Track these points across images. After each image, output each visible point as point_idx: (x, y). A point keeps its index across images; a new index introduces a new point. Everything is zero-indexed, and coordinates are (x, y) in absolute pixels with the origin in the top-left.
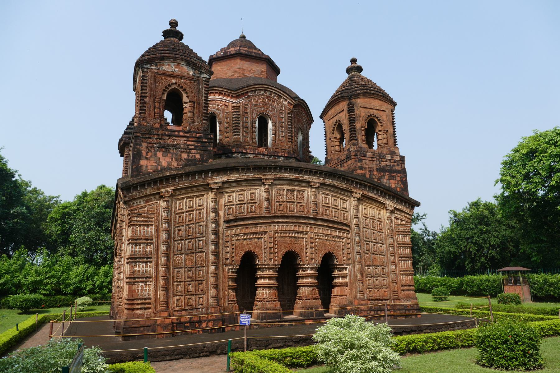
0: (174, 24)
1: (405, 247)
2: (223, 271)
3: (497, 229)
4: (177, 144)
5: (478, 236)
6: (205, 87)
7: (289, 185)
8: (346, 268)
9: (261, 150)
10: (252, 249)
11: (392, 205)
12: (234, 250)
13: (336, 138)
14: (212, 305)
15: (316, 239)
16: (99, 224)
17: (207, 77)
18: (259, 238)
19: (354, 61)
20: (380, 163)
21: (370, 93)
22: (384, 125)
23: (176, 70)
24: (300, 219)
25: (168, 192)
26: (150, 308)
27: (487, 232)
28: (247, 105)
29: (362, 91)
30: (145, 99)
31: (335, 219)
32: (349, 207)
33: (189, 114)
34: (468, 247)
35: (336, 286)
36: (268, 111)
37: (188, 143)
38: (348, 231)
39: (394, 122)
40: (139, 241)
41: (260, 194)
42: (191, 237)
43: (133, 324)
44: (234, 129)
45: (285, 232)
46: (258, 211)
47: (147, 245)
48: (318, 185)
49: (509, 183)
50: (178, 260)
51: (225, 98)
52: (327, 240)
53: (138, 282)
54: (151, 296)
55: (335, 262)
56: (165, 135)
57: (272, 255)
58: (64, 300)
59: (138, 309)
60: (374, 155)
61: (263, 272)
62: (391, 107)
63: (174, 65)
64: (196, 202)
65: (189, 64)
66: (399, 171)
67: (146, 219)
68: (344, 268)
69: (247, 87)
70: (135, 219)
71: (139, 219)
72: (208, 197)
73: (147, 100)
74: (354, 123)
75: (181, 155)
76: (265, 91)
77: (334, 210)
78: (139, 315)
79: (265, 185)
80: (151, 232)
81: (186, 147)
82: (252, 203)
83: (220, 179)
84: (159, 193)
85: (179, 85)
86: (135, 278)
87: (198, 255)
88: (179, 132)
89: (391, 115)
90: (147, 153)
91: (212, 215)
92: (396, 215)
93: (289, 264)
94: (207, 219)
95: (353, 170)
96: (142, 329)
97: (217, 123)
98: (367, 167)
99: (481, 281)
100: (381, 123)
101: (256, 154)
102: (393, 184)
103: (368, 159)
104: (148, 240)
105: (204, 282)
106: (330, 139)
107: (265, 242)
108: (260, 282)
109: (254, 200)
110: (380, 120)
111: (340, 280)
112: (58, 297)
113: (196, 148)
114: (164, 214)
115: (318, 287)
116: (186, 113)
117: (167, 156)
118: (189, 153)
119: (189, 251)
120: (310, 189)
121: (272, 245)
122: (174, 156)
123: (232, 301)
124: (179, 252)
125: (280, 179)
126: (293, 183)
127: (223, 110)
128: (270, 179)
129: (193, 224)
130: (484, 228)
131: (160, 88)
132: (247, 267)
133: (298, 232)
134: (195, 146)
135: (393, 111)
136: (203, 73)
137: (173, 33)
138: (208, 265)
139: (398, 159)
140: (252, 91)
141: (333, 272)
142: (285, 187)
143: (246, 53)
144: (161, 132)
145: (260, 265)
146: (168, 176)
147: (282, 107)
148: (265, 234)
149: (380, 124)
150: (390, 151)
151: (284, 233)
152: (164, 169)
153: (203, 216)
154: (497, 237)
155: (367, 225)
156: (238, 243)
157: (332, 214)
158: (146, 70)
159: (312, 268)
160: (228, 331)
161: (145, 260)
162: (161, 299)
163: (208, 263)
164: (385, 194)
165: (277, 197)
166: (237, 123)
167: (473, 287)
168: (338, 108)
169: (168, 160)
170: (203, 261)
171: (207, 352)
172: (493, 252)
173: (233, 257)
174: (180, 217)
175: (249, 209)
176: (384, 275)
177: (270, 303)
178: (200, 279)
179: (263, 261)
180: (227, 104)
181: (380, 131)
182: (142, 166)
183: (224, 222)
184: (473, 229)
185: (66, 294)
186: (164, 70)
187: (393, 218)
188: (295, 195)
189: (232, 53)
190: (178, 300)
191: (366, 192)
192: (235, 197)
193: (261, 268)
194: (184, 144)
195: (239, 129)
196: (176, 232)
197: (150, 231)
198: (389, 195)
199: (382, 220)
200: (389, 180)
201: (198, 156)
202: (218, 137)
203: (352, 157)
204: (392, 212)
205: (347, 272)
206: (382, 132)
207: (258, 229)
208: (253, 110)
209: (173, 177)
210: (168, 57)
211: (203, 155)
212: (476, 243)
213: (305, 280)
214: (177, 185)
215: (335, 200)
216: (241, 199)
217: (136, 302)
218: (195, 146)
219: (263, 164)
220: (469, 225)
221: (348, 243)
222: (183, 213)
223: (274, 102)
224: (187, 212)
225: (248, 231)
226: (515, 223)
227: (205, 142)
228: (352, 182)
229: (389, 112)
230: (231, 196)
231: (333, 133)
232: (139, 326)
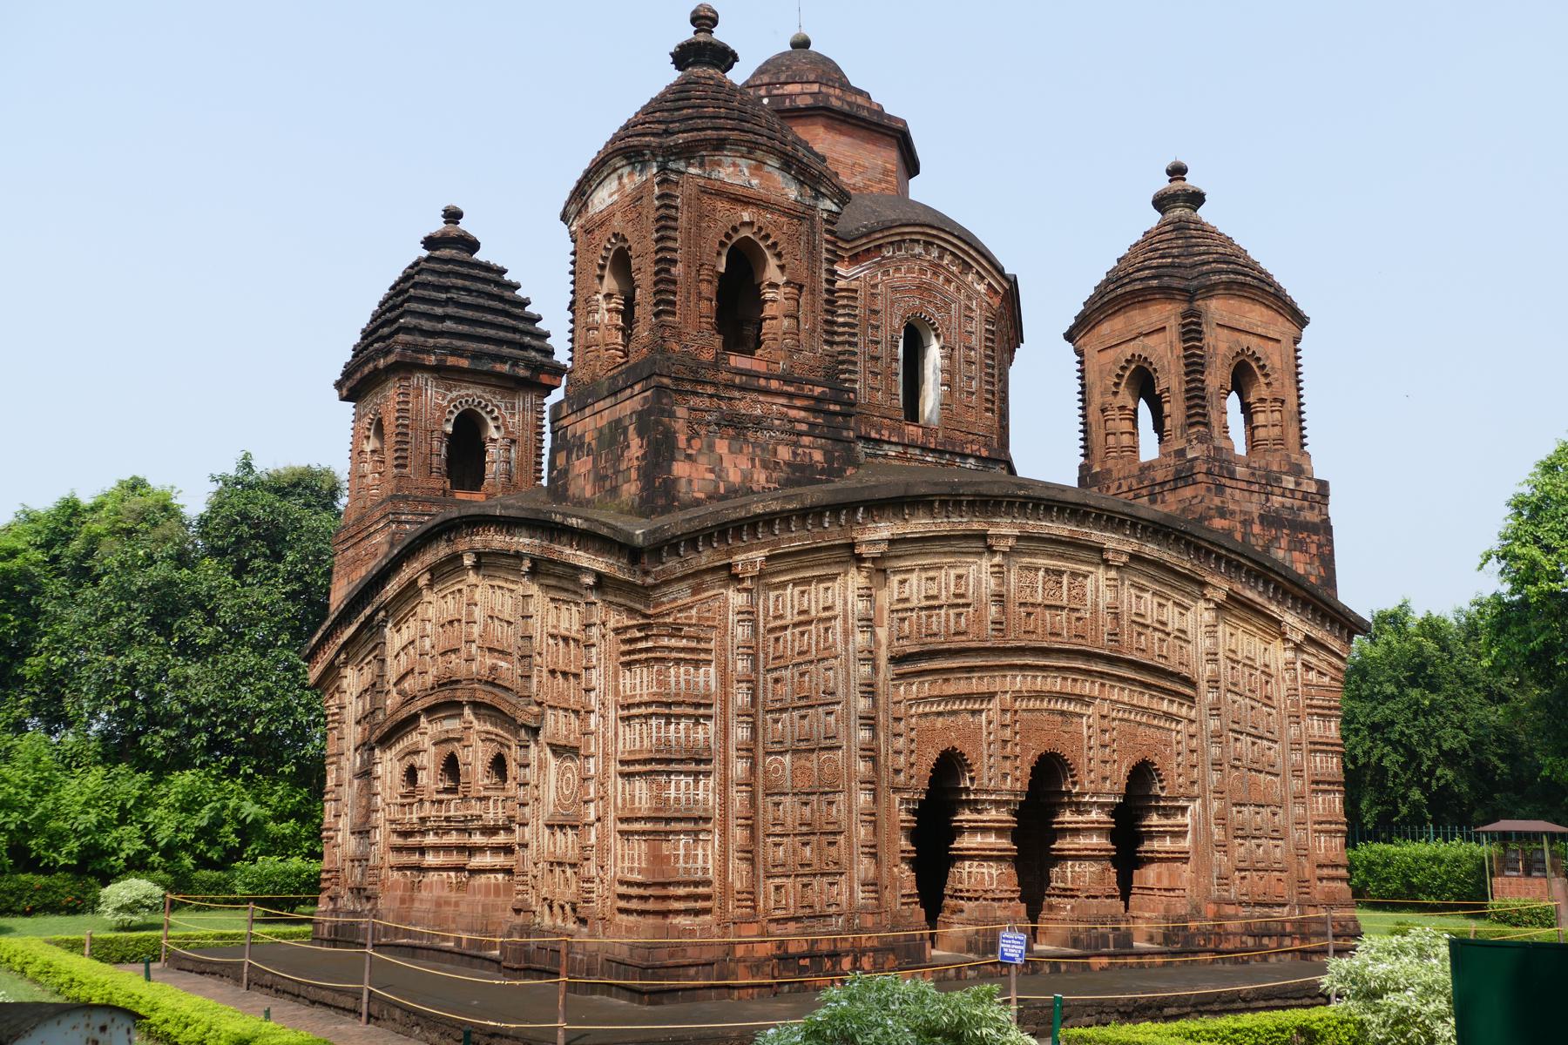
0: (704, 20)
1: (1326, 752)
2: (889, 809)
3: (1460, 700)
5: (1407, 720)
6: (827, 241)
7: (1051, 556)
8: (1184, 809)
9: (912, 430)
10: (956, 744)
11: (1299, 625)
12: (913, 747)
13: (1122, 408)
14: (865, 907)
16: (161, 621)
17: (834, 208)
18: (974, 712)
20: (1267, 500)
21: (1244, 284)
22: (1276, 384)
23: (755, 182)
24: (1075, 659)
25: (753, 563)
26: (707, 911)
27: (1434, 709)
28: (875, 286)
31: (1161, 663)
32: (1195, 630)
33: (786, 322)
34: (1377, 753)
35: (1152, 860)
36: (931, 309)
37: (793, 413)
38: (1191, 699)
39: (1298, 374)
40: (675, 710)
41: (979, 581)
42: (806, 704)
43: (671, 956)
45: (1039, 695)
46: (974, 629)
47: (697, 723)
48: (1125, 559)
49: (1534, 565)
50: (776, 770)
52: (1140, 724)
53: (677, 833)
54: (710, 875)
55: (1156, 790)
56: (735, 387)
58: (46, 889)
59: (678, 912)
61: (979, 812)
62: (1293, 330)
63: (749, 167)
64: (816, 598)
66: (1314, 524)
67: (694, 644)
69: (881, 231)
70: (665, 642)
71: (673, 642)
73: (678, 270)
75: (775, 453)
76: (927, 244)
77: (1158, 635)
78: (684, 932)
80: (706, 683)
81: (788, 426)
82: (958, 606)
83: (884, 530)
84: (729, 565)
85: (760, 229)
86: (668, 820)
87: (825, 755)
90: (689, 440)
91: (861, 639)
92: (1305, 656)
94: (847, 650)
95: (1202, 518)
96: (692, 971)
98: (1237, 508)
99: (1416, 860)
100: (1266, 375)
101: (904, 445)
102: (1301, 565)
104: (698, 705)
105: (841, 839)
106: (1103, 411)
107: (990, 723)
108: (966, 842)
111: (1168, 844)
112: (23, 877)
114: (741, 632)
115: (1113, 860)
118: (796, 444)
119: (803, 745)
120: (1101, 570)
121: (1008, 733)
124: (777, 747)
125: (1030, 538)
126: (1061, 549)
128: (1006, 537)
129: (811, 662)
130: (1423, 696)
131: (713, 236)
134: (811, 425)
135: (1297, 341)
136: (824, 195)
138: (850, 788)
140: (892, 243)
141: (1142, 817)
142: (1041, 561)
143: (846, 107)
145: (976, 791)
146: (760, 515)
147: (969, 298)
149: (1262, 380)
150: (1290, 463)
152: (732, 492)
153: (834, 645)
154: (1461, 727)
155: (1235, 685)
156: (924, 723)
157: (1151, 648)
158: (673, 177)
159: (1101, 806)
161: (693, 767)
162: (738, 886)
163: (849, 781)
165: (1021, 589)
166: (850, 344)
167: (1386, 880)
168: (1142, 318)
170: (836, 775)
172: (1450, 774)
173: (912, 765)
174: (777, 639)
175: (952, 624)
176: (1277, 834)
177: (1003, 904)
178: (831, 828)
179: (985, 781)
181: (1262, 400)
184: (1393, 696)
185: (48, 870)
187: (1299, 665)
190: (778, 888)
191: (1238, 587)
192: (916, 587)
193: (976, 802)
194: (783, 417)
195: (855, 363)
196: (770, 686)
197: (701, 680)
198: (1295, 598)
199: (1273, 671)
200: (1290, 550)
201: (818, 456)
203: (1200, 477)
205: (1188, 820)
206: (1268, 404)
207: (976, 685)
208: (893, 303)
209: (768, 520)
210: (737, 142)
211: (831, 452)
212: (1399, 741)
213: (1082, 841)
214: (776, 544)
215: (1160, 605)
216: (931, 593)
217: (672, 891)
218: (811, 425)
219: (996, 491)
220: (1380, 684)
221: (1192, 736)
222: (785, 628)
223: (948, 281)
224: (795, 625)
225: (951, 689)
226: (1509, 685)
227: (835, 413)
228: (1208, 553)
229: (1286, 342)
231: (1115, 393)
232: (686, 961)
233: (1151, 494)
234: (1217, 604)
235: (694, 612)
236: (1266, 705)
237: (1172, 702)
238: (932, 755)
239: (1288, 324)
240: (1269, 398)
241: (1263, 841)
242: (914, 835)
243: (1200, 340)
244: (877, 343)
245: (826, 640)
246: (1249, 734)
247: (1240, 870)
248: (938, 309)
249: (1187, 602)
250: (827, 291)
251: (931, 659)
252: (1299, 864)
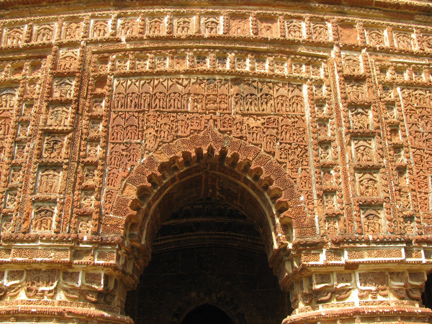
57: (59, 179)
133: (255, 48)
148: (35, 67)
151: (159, 52)
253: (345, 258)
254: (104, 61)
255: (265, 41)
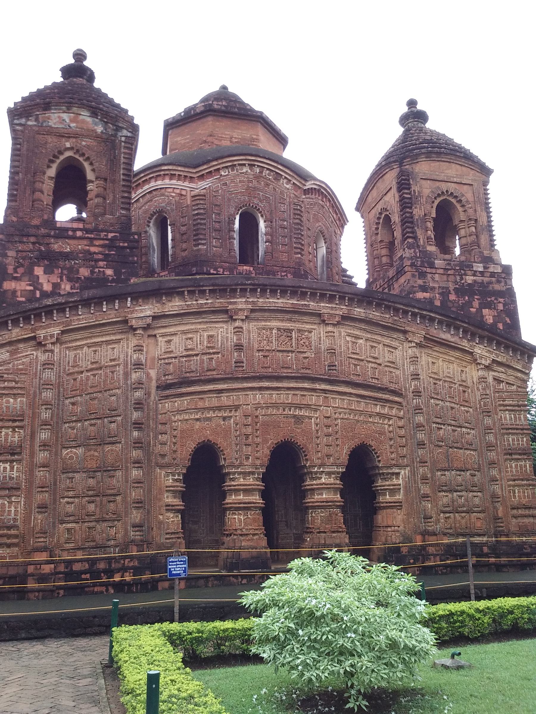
0: (80, 56)
1: (517, 434)
4: (71, 252)
8: (398, 474)
10: (211, 438)
11: (488, 355)
15: (336, 419)
17: (129, 134)
18: (224, 419)
19: (412, 103)
20: (462, 279)
22: (470, 211)
23: (73, 125)
25: (52, 336)
29: (423, 151)
30: (16, 178)
36: (256, 201)
37: (93, 249)
38: (400, 403)
44: (195, 235)
45: (275, 405)
48: (337, 319)
50: (71, 458)
51: (180, 183)
52: (358, 421)
56: (49, 236)
57: (250, 448)
60: (449, 264)
64: (106, 354)
65: (94, 114)
68: (393, 474)
69: (216, 159)
72: (127, 344)
74: (411, 208)
75: (78, 272)
76: (251, 166)
77: (370, 365)
79: (236, 320)
82: (209, 353)
83: (147, 310)
84: (34, 338)
85: (78, 151)
87: (108, 448)
88: (74, 230)
89: (482, 191)
91: (135, 376)
92: (495, 374)
93: (285, 467)
95: (409, 293)
97: (169, 227)
98: (436, 285)
100: (463, 206)
103: (438, 271)
105: (119, 498)
107: (237, 425)
108: (231, 499)
109: (213, 348)
110: (460, 201)
113: (106, 258)
116: (91, 199)
117: (52, 272)
121: (249, 430)
122: (65, 272)
123: (172, 533)
126: (288, 316)
127: (178, 203)
132: (205, 470)
135: (485, 183)
137: (78, 72)
138: (127, 467)
139: (499, 270)
140: (226, 167)
143: (223, 108)
144: (43, 231)
146: (49, 306)
149: (460, 209)
159: (329, 474)
160: (164, 589)
161: (9, 457)
164: (473, 335)
166: (201, 224)
168: (382, 186)
169: (55, 279)
171: (99, 626)
175: (205, 365)
178: (113, 491)
180: (184, 193)
182: (6, 291)
183: (158, 387)
186: (51, 127)
187: (490, 380)
188: (294, 339)
189: (198, 111)
193: (229, 474)
198: (481, 338)
199: (469, 384)
201: (109, 272)
202: (170, 252)
203: (406, 269)
204: (488, 368)
205: (401, 482)
207: (225, 400)
208: (229, 200)
216: (189, 347)
222: (82, 372)
227: (124, 248)
228: (405, 312)
230: (169, 342)
231: (377, 234)
233: (389, 286)
234: (416, 344)
235: (11, 366)
236: (464, 406)
237: (383, 407)
238: (191, 446)
239: (478, 174)
240: (467, 220)
241: (464, 493)
242: (184, 496)
243: (409, 189)
244: (219, 222)
245: (113, 378)
246: (448, 425)
247: (444, 512)
248: (261, 201)
249: (395, 344)
250: (124, 180)
251: (189, 387)
252: (495, 508)
253: (321, 470)
254: (257, 410)
255: (303, 404)
